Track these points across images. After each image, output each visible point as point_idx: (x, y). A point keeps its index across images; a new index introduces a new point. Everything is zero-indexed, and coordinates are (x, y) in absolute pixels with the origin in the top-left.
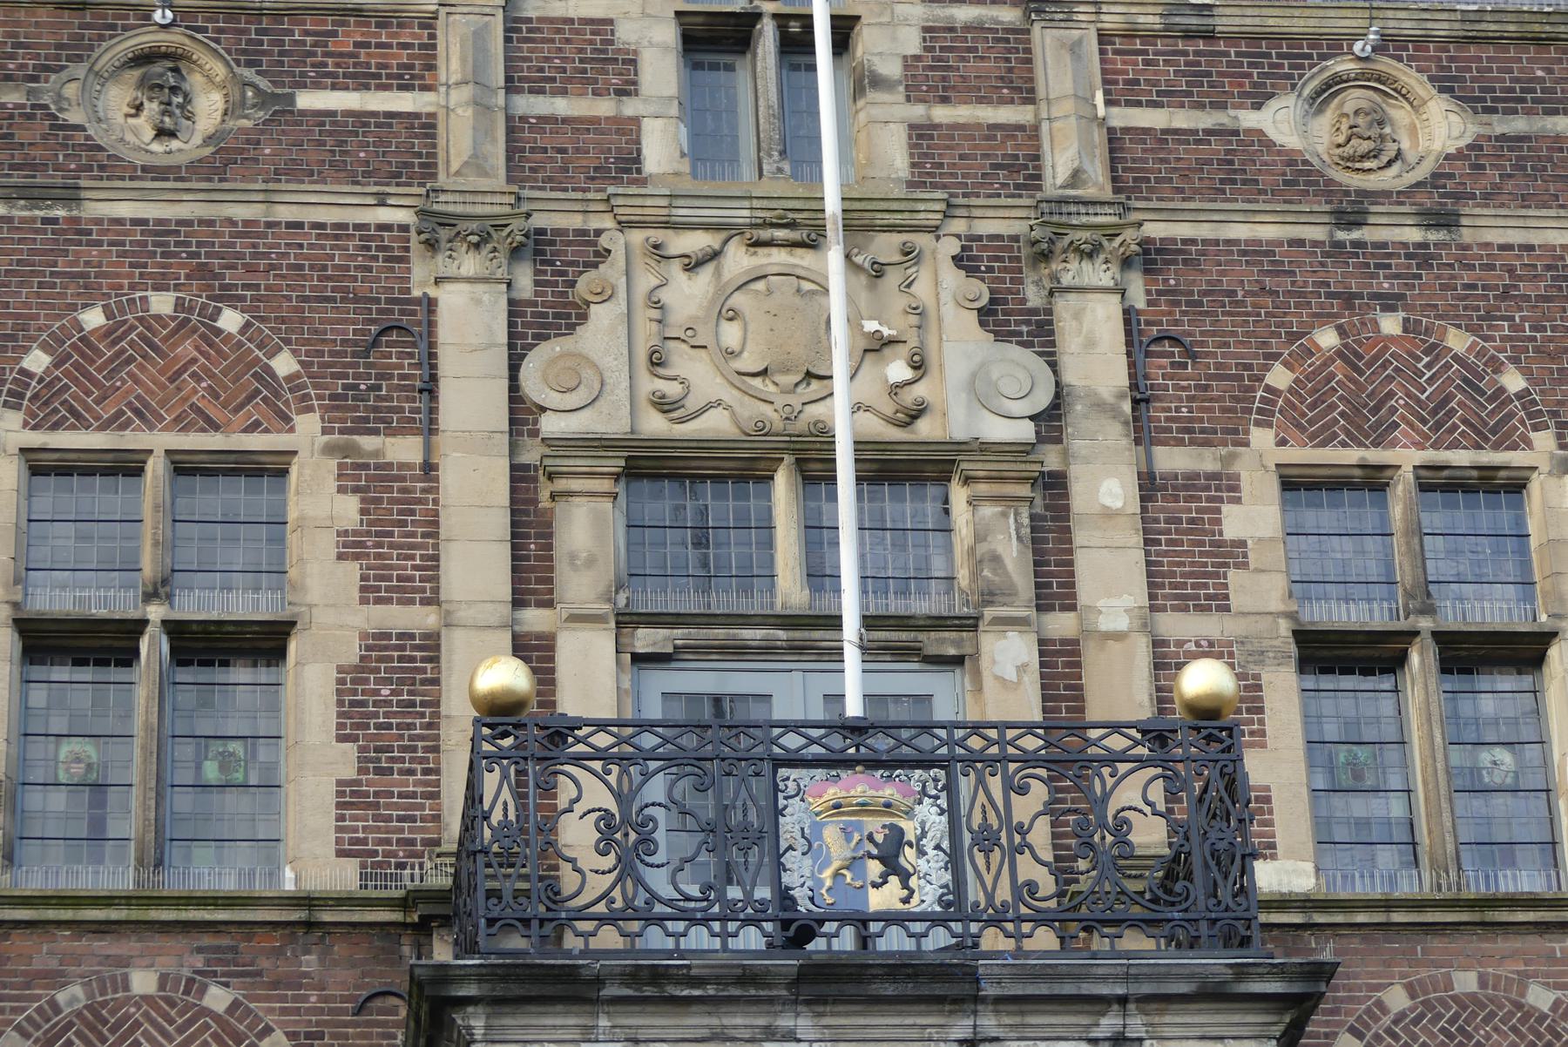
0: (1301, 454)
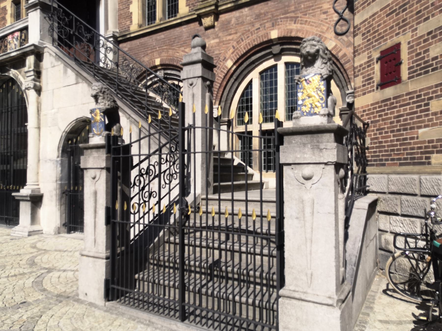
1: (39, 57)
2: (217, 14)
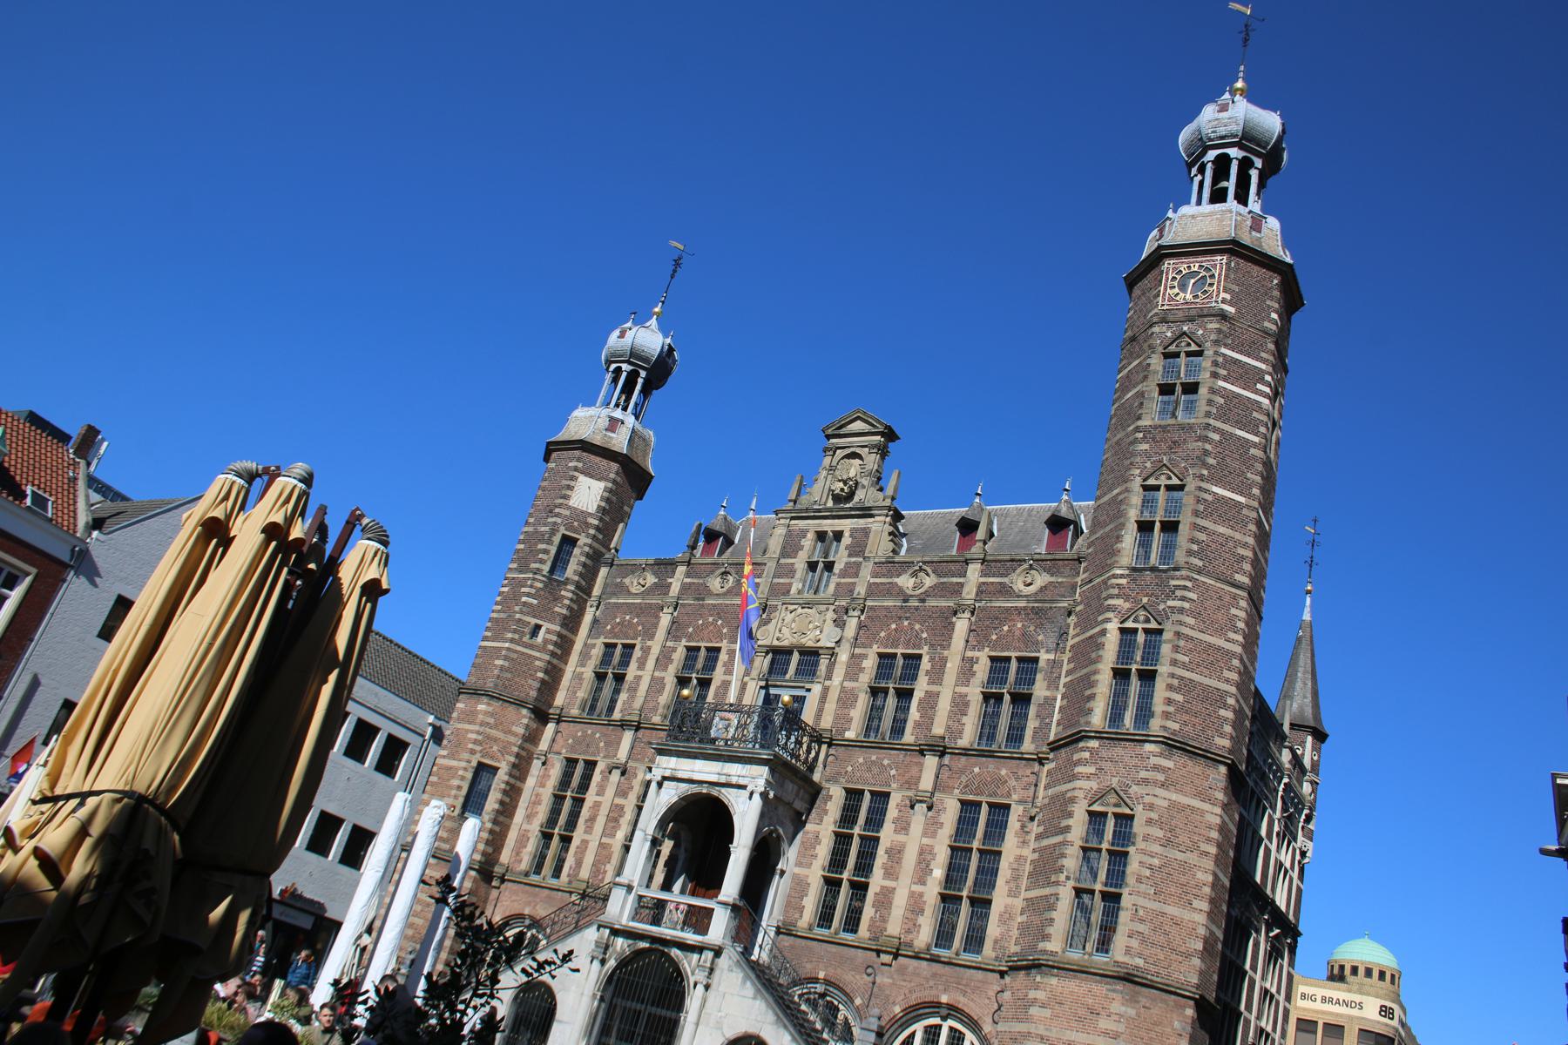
1: (718, 952)
2: (896, 956)
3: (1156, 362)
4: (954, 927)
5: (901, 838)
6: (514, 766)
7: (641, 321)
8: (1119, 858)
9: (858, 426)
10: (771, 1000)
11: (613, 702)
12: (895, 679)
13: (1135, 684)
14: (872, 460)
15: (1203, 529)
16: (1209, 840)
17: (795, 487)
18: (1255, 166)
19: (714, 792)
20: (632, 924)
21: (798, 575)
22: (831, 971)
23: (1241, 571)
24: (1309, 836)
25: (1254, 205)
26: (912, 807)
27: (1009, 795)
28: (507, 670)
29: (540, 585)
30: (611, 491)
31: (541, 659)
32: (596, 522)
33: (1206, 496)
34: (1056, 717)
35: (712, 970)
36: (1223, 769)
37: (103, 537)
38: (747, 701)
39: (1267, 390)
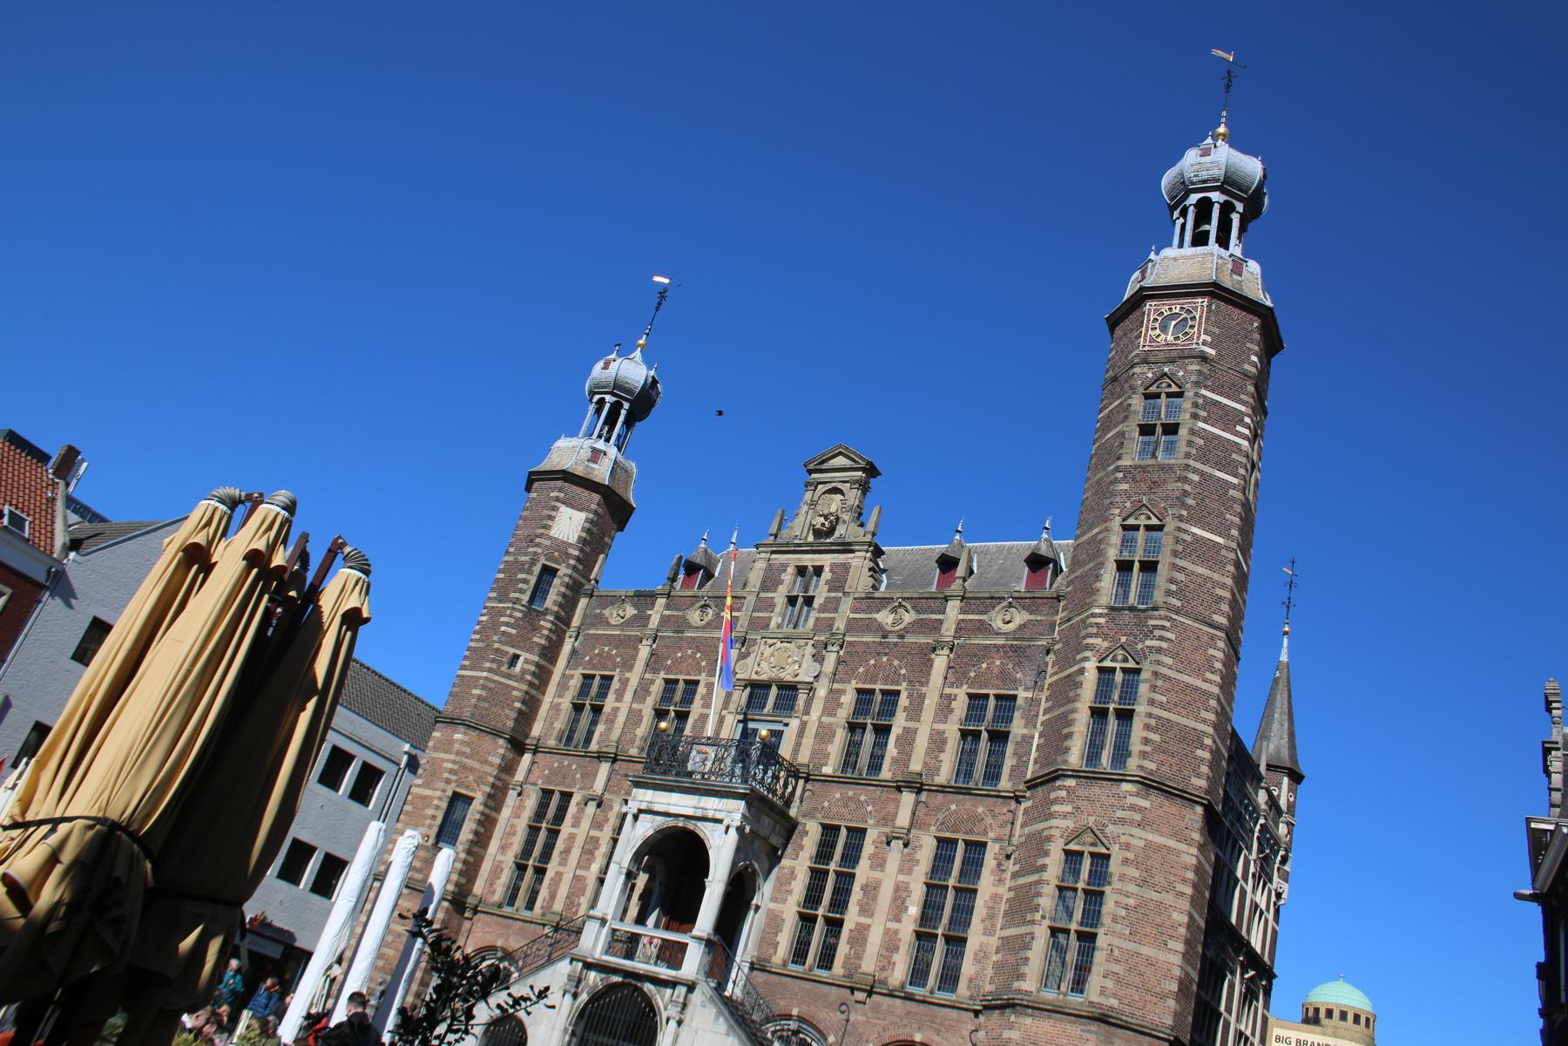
0: (861, 686)
1: (691, 988)
2: (870, 993)
3: (1137, 402)
4: (929, 965)
5: (877, 874)
6: (489, 796)
7: (625, 353)
8: (1094, 897)
9: (840, 461)
10: (743, 1036)
11: (590, 733)
12: (873, 715)
13: (1112, 723)
14: (853, 496)
15: (1182, 569)
16: (1184, 880)
17: (777, 520)
18: (1235, 210)
19: (691, 825)
20: (605, 958)
21: (778, 609)
22: (805, 1008)
23: (1219, 611)
24: (1285, 877)
25: (1236, 248)
26: (888, 843)
27: (985, 833)
28: (484, 699)
29: (519, 615)
30: (592, 522)
31: (519, 689)
32: (576, 553)
33: (1186, 537)
34: (1034, 755)
35: (684, 1005)
36: (1199, 810)
37: (79, 559)
38: (725, 734)
39: (1247, 432)
